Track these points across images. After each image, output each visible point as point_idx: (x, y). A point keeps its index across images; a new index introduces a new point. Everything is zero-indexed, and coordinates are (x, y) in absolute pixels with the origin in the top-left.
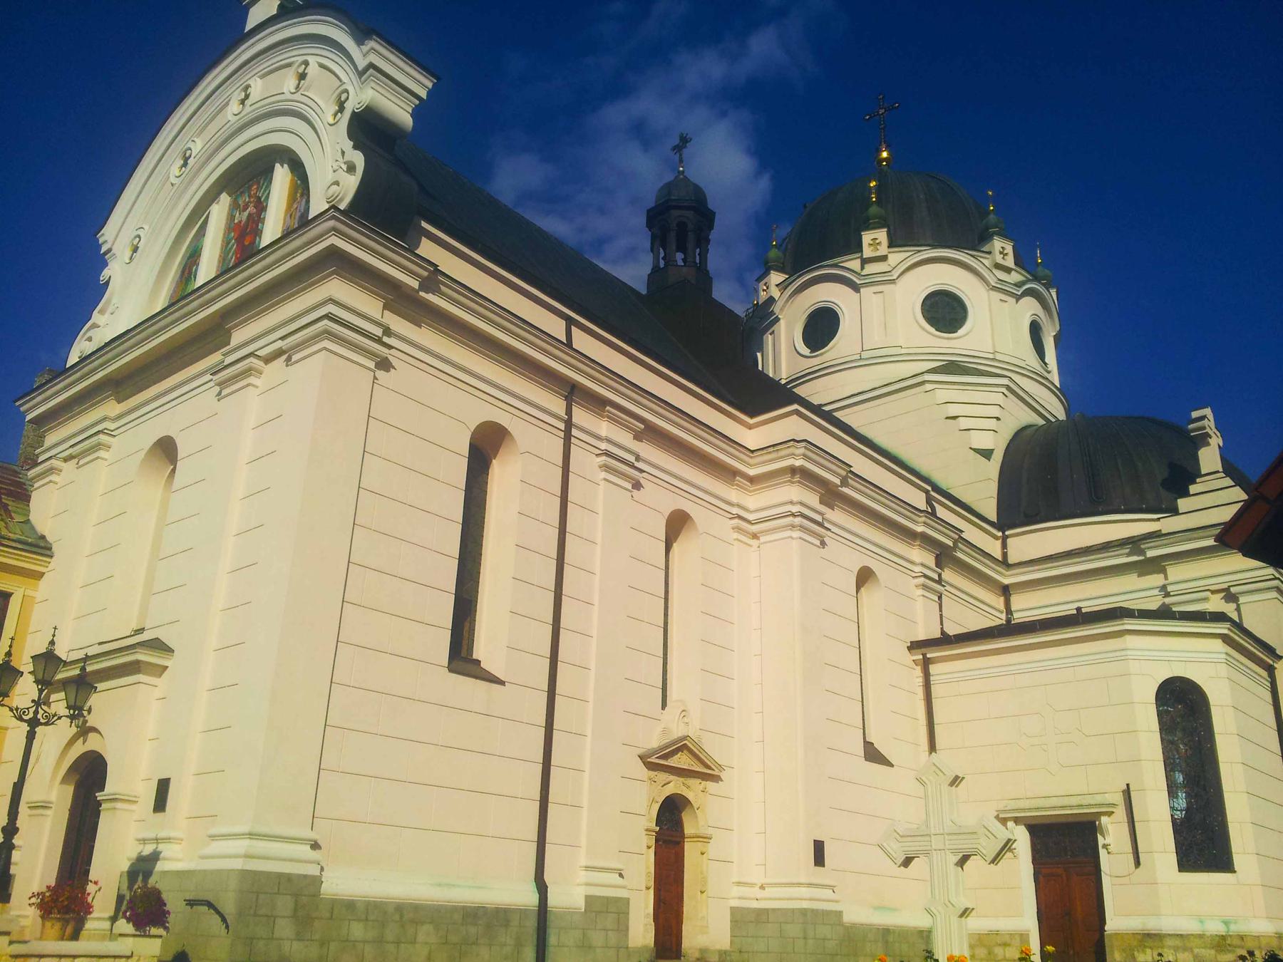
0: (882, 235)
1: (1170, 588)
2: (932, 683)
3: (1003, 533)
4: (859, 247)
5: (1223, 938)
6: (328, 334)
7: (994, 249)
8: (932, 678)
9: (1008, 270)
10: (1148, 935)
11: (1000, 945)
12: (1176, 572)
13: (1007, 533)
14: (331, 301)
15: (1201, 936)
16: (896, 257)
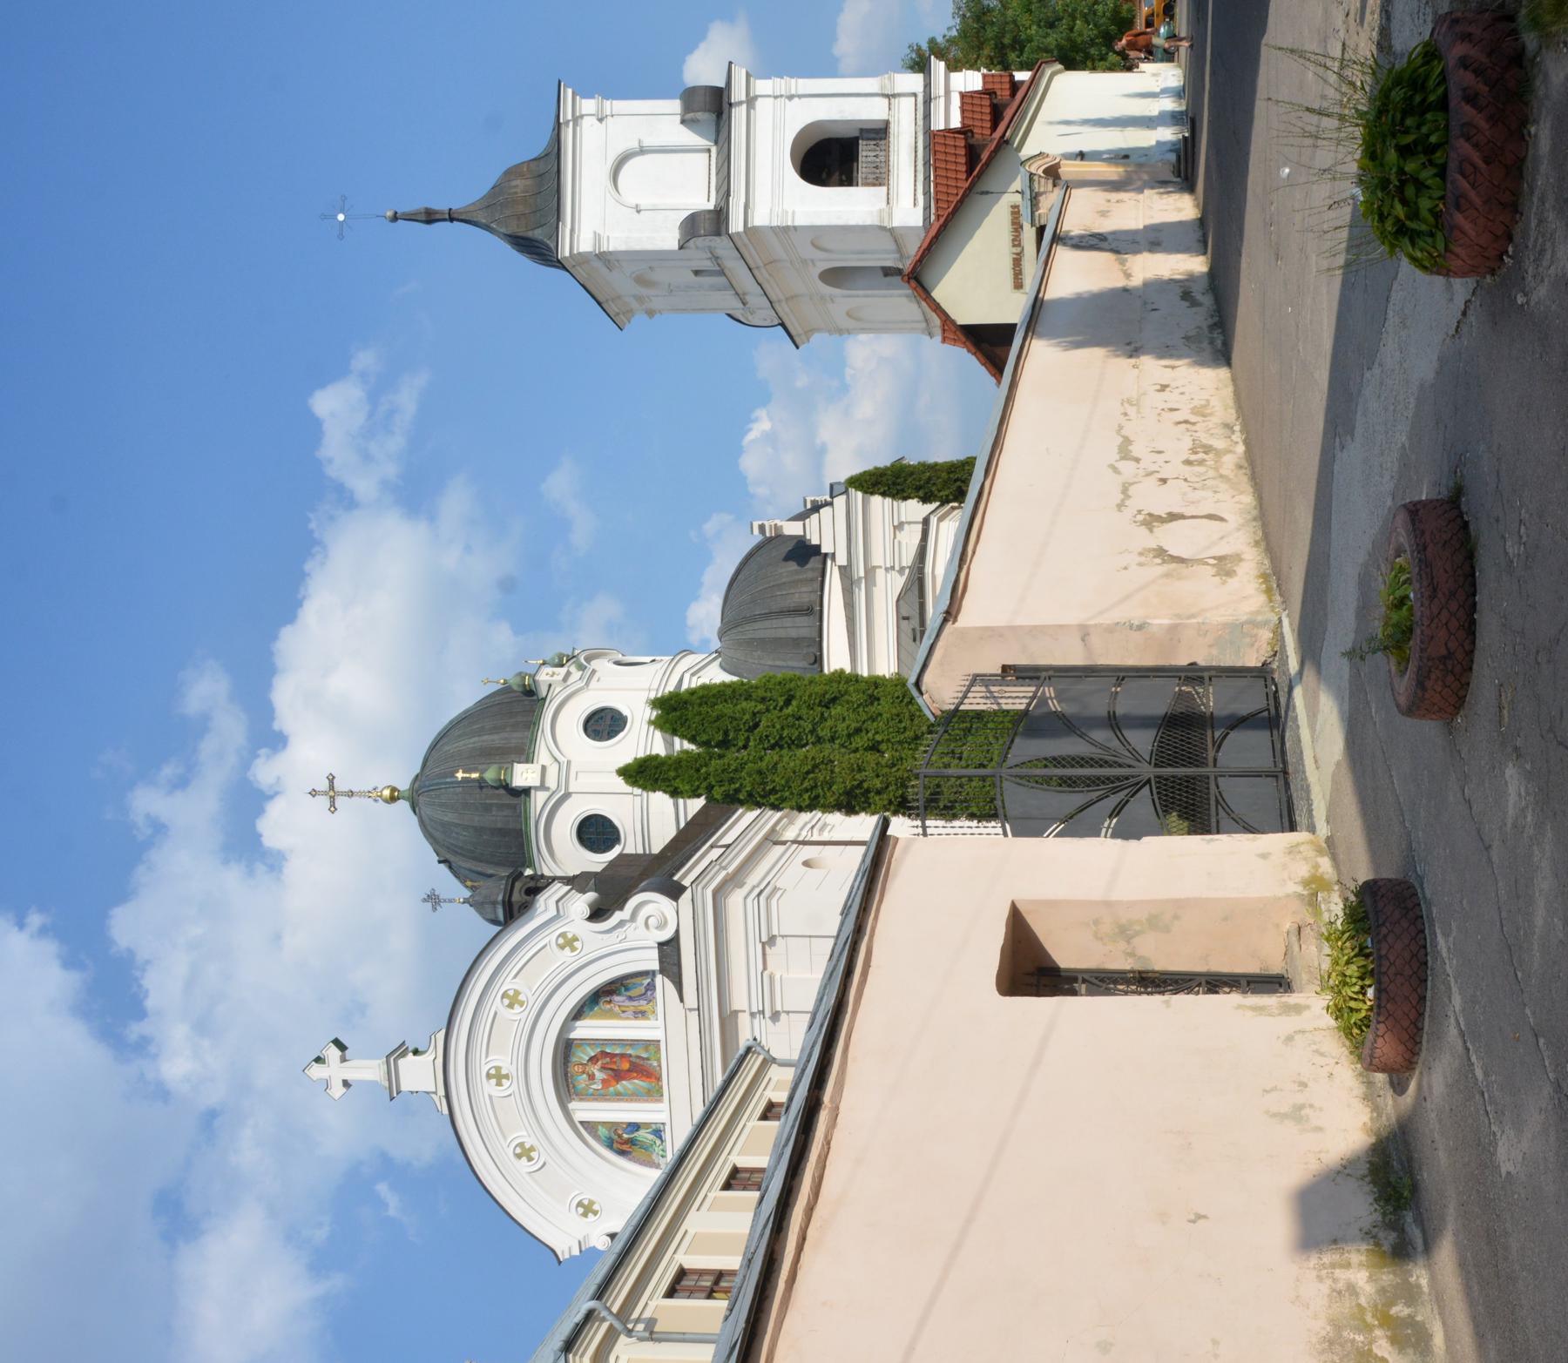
1: (888, 566)
4: (526, 791)
6: (768, 898)
9: (568, 674)
12: (877, 559)
14: (746, 898)
16: (543, 755)
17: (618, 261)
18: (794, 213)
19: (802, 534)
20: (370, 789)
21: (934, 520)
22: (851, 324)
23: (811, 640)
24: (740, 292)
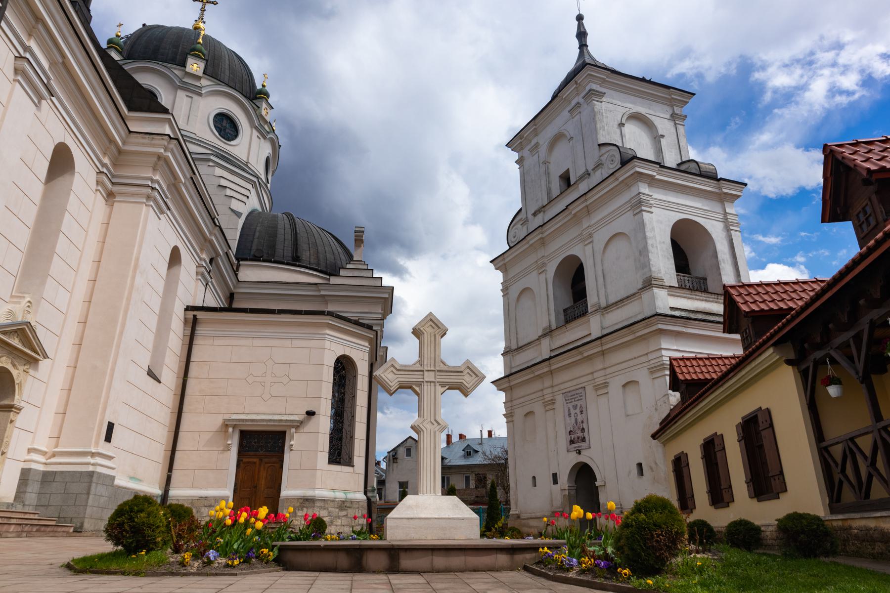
0: (202, 65)
2: (195, 335)
3: (239, 262)
4: (183, 64)
5: (343, 502)
7: (262, 105)
8: (196, 332)
10: (307, 500)
11: (206, 506)
13: (241, 263)
15: (333, 501)
17: (580, 112)
18: (651, 213)
19: (354, 259)
20: (204, 20)
21: (371, 335)
22: (515, 291)
23: (274, 256)
24: (547, 208)
